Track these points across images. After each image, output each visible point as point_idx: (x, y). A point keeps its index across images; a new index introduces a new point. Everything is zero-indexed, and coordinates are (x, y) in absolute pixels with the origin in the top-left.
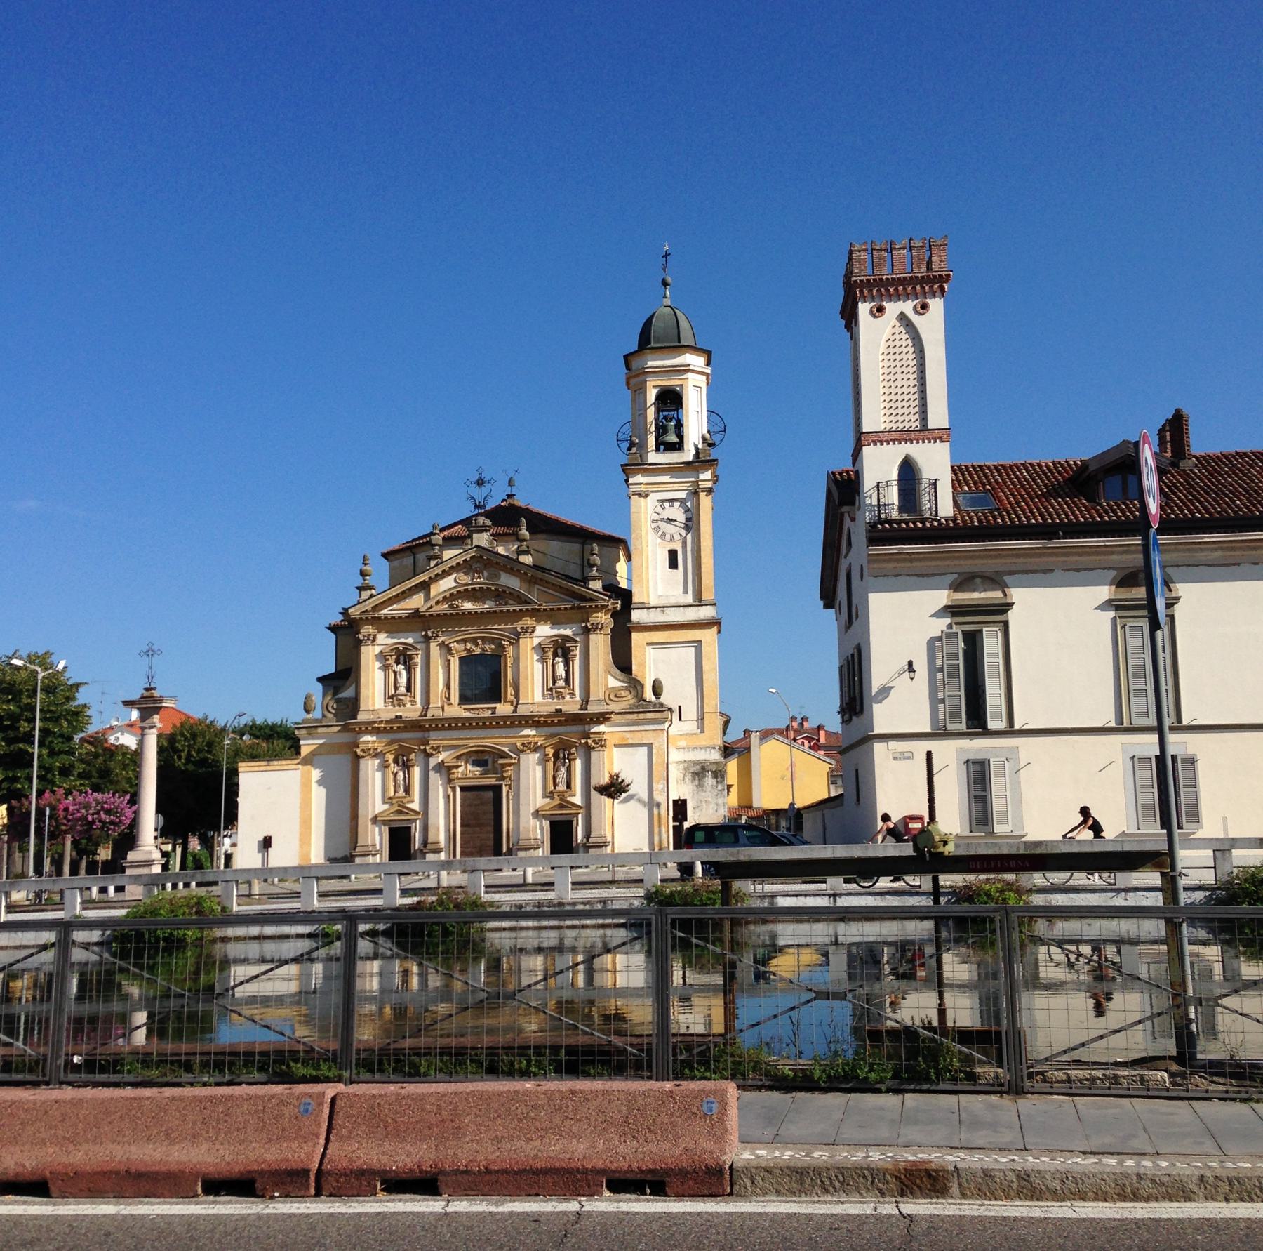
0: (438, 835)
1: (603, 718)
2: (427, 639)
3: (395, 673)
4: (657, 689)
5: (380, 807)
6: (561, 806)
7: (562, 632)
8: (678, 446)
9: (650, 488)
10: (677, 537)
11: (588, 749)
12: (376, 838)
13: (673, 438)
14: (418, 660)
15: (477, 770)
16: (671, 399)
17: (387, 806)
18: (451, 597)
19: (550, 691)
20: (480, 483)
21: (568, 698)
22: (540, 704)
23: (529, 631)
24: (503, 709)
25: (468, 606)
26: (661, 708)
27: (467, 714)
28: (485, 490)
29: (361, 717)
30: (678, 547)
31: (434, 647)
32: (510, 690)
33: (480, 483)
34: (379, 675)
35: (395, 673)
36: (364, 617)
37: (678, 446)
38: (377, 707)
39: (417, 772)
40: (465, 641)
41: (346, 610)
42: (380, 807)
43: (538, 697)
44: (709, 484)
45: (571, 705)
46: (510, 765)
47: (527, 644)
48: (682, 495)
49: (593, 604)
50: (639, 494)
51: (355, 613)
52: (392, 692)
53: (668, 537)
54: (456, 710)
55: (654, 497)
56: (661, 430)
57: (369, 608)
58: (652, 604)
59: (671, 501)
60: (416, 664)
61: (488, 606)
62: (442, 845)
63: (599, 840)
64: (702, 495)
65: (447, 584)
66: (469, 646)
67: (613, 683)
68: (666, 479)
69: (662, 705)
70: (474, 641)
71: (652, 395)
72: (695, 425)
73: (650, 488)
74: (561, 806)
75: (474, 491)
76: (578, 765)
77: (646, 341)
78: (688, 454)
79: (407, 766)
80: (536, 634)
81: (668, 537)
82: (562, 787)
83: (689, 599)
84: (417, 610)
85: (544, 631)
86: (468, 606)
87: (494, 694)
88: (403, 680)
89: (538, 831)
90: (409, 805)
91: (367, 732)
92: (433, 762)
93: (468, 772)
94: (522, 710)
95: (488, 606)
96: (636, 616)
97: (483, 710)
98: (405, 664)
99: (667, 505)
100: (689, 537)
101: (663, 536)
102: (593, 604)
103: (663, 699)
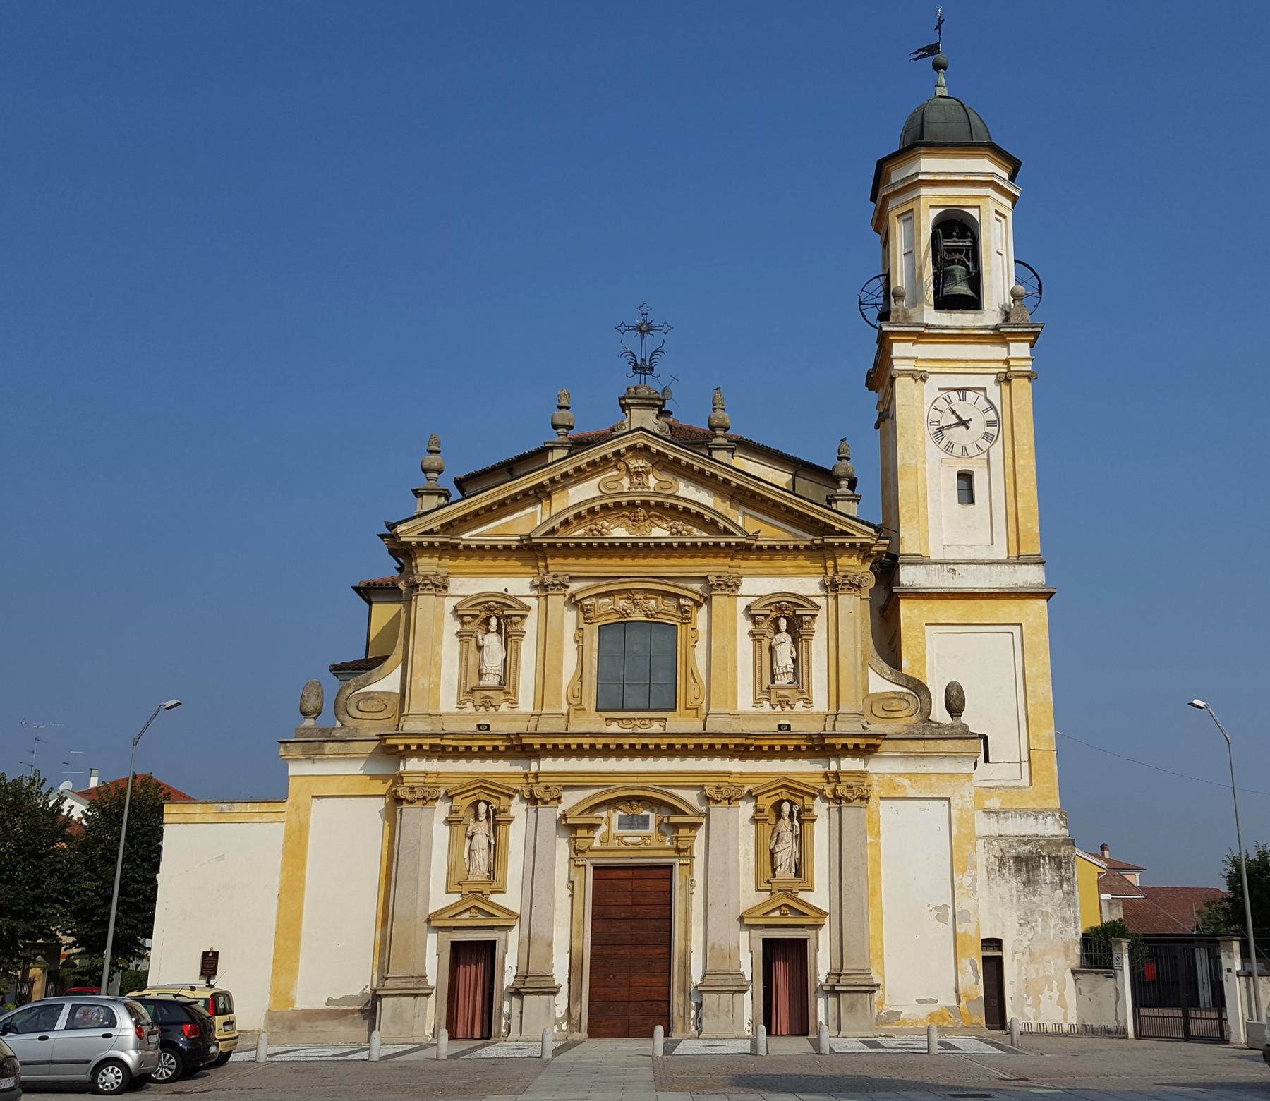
4: (955, 704)
5: (439, 899)
8: (973, 303)
9: (926, 366)
10: (972, 450)
13: (963, 289)
16: (957, 232)
17: (456, 898)
19: (764, 692)
23: (732, 586)
24: (679, 722)
27: (615, 728)
28: (653, 342)
33: (645, 330)
34: (450, 651)
36: (425, 540)
37: (973, 303)
38: (443, 708)
41: (392, 526)
43: (745, 702)
44: (1027, 366)
45: (812, 713)
50: (911, 374)
51: (409, 533)
53: (957, 450)
54: (592, 722)
56: (941, 277)
57: (435, 526)
58: (933, 558)
60: (522, 634)
62: (561, 976)
63: (861, 980)
65: (584, 492)
66: (622, 603)
67: (879, 684)
69: (965, 727)
72: (999, 278)
75: (633, 342)
76: (820, 832)
77: (917, 141)
78: (990, 316)
81: (957, 450)
85: (759, 585)
86: (620, 532)
90: (494, 898)
93: (616, 838)
95: (659, 532)
96: (908, 576)
98: (499, 632)
99: (954, 395)
101: (950, 447)
102: (847, 541)
103: (965, 718)
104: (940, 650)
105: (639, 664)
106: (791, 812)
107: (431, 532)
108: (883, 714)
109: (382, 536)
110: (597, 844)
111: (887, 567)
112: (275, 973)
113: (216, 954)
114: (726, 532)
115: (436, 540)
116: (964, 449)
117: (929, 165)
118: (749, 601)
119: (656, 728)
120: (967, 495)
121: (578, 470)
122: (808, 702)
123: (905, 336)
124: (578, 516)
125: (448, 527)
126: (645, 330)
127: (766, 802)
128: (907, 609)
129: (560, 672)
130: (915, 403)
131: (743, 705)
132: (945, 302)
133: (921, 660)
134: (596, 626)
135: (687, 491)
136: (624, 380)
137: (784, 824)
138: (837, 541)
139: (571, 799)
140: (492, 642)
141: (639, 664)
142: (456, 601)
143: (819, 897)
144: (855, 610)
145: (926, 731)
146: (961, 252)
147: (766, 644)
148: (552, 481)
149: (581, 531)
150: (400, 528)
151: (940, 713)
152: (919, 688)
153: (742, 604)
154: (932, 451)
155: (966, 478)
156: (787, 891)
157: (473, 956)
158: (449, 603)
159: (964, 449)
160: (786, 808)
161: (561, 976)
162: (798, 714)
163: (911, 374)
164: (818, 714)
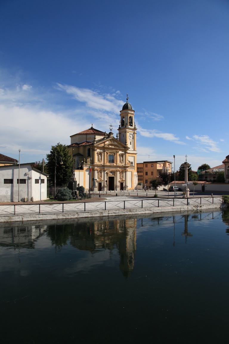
1: (128, 167)
2: (104, 151)
6: (122, 181)
11: (126, 172)
14: (103, 155)
15: (111, 174)
18: (108, 145)
24: (115, 164)
25: (110, 146)
27: (110, 165)
29: (95, 164)
31: (105, 153)
32: (116, 161)
40: (109, 152)
47: (118, 154)
48: (132, 133)
50: (128, 132)
54: (108, 164)
55: (129, 133)
59: (131, 134)
64: (135, 134)
68: (131, 131)
71: (129, 116)
74: (122, 181)
79: (101, 173)
83: (133, 150)
85: (120, 152)
86: (110, 146)
89: (119, 184)
91: (96, 166)
92: (105, 172)
93: (111, 175)
94: (118, 165)
97: (112, 164)
119: (113, 165)
122: (123, 163)
123: (127, 129)
126: (111, 126)
130: (128, 134)
131: (119, 164)
140: (100, 156)
151: (131, 165)
155: (131, 142)
160: (122, 172)
163: (128, 132)
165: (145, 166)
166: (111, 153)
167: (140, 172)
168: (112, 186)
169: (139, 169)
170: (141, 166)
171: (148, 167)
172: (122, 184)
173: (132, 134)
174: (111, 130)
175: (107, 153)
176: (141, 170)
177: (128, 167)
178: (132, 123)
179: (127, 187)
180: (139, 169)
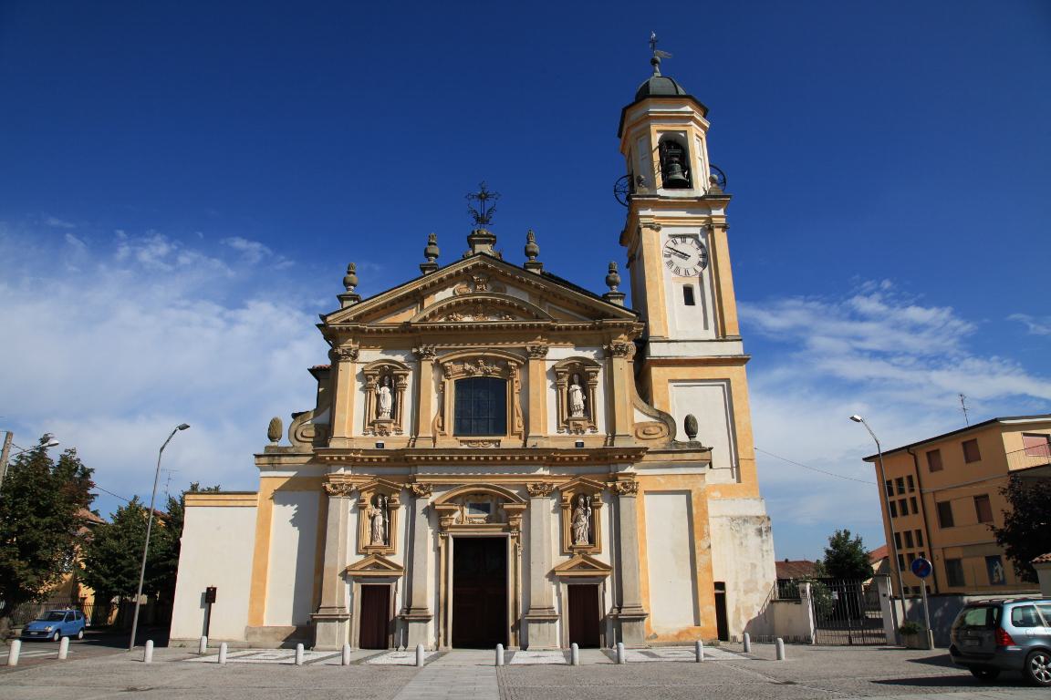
0: (424, 598)
1: (634, 455)
2: (418, 358)
3: (378, 396)
5: (352, 558)
6: (583, 566)
7: (580, 354)
9: (662, 222)
10: (692, 272)
11: (615, 497)
12: (346, 597)
14: (409, 381)
15: (480, 517)
17: (362, 557)
18: (448, 310)
19: (566, 422)
20: (483, 197)
21: (588, 432)
22: (555, 439)
26: (699, 449)
27: (465, 447)
28: (489, 204)
29: (333, 444)
30: (688, 281)
31: (426, 366)
32: (518, 421)
33: (483, 197)
34: (359, 398)
35: (378, 396)
37: (687, 184)
38: (354, 435)
39: (401, 514)
40: (462, 361)
42: (352, 558)
43: (552, 430)
44: (723, 221)
46: (519, 511)
47: (539, 369)
48: (697, 231)
49: (618, 322)
50: (651, 226)
52: (374, 417)
53: (682, 272)
54: (449, 441)
55: (665, 232)
56: (666, 170)
57: (351, 317)
58: (671, 339)
59: (684, 237)
60: (404, 387)
61: (492, 320)
62: (431, 610)
64: (717, 232)
66: (468, 367)
67: (640, 417)
68: (683, 214)
69: (698, 444)
70: (474, 361)
71: (656, 139)
73: (662, 222)
74: (583, 566)
76: (604, 513)
79: (388, 510)
80: (547, 357)
81: (682, 272)
82: (583, 542)
83: (711, 334)
84: (408, 323)
85: (560, 353)
87: (501, 428)
88: (387, 404)
89: (553, 597)
90: (388, 558)
91: (340, 463)
92: (421, 504)
95: (492, 320)
96: (656, 350)
97: (485, 442)
98: (390, 386)
99: (679, 240)
100: (706, 273)
101: (677, 271)
102: (618, 322)
103: (698, 438)
104: (676, 397)
105: (484, 404)
106: (586, 502)
107: (348, 321)
108: (645, 436)
109: (319, 326)
110: (454, 523)
111: (642, 343)
112: (251, 602)
113: (215, 589)
114: (537, 318)
115: (350, 326)
116: (686, 272)
117: (654, 109)
118: (554, 363)
119: (492, 446)
120: (689, 297)
121: (441, 280)
122: (594, 428)
123: (647, 205)
124: (441, 310)
125: (358, 318)
127: (568, 496)
128: (656, 373)
129: (429, 409)
130: (655, 244)
132: (669, 184)
133: (666, 403)
134: (453, 381)
135: (511, 292)
136: (469, 226)
137: (580, 511)
138: (611, 322)
139: (435, 497)
140: (385, 391)
141: (484, 404)
142: (363, 365)
143: (605, 557)
144: (623, 368)
145: (673, 448)
146: (677, 156)
147: (565, 390)
148: (425, 288)
149: (442, 320)
150: (329, 319)
151: (681, 436)
152: (665, 418)
153: (549, 365)
154: (667, 273)
156: (583, 552)
157: (375, 598)
158: (358, 368)
159: (686, 272)
160: (580, 502)
161: (431, 610)
162: (588, 437)
164: (602, 437)
165: (923, 461)
166: (474, 361)
167: (905, 512)
168: (482, 613)
169: (906, 487)
170: (904, 469)
171: (944, 467)
172: (583, 599)
173: (695, 237)
174: (478, 220)
175: (441, 368)
176: (907, 496)
177: (634, 455)
178: (686, 167)
179: (640, 618)
180: (906, 487)
